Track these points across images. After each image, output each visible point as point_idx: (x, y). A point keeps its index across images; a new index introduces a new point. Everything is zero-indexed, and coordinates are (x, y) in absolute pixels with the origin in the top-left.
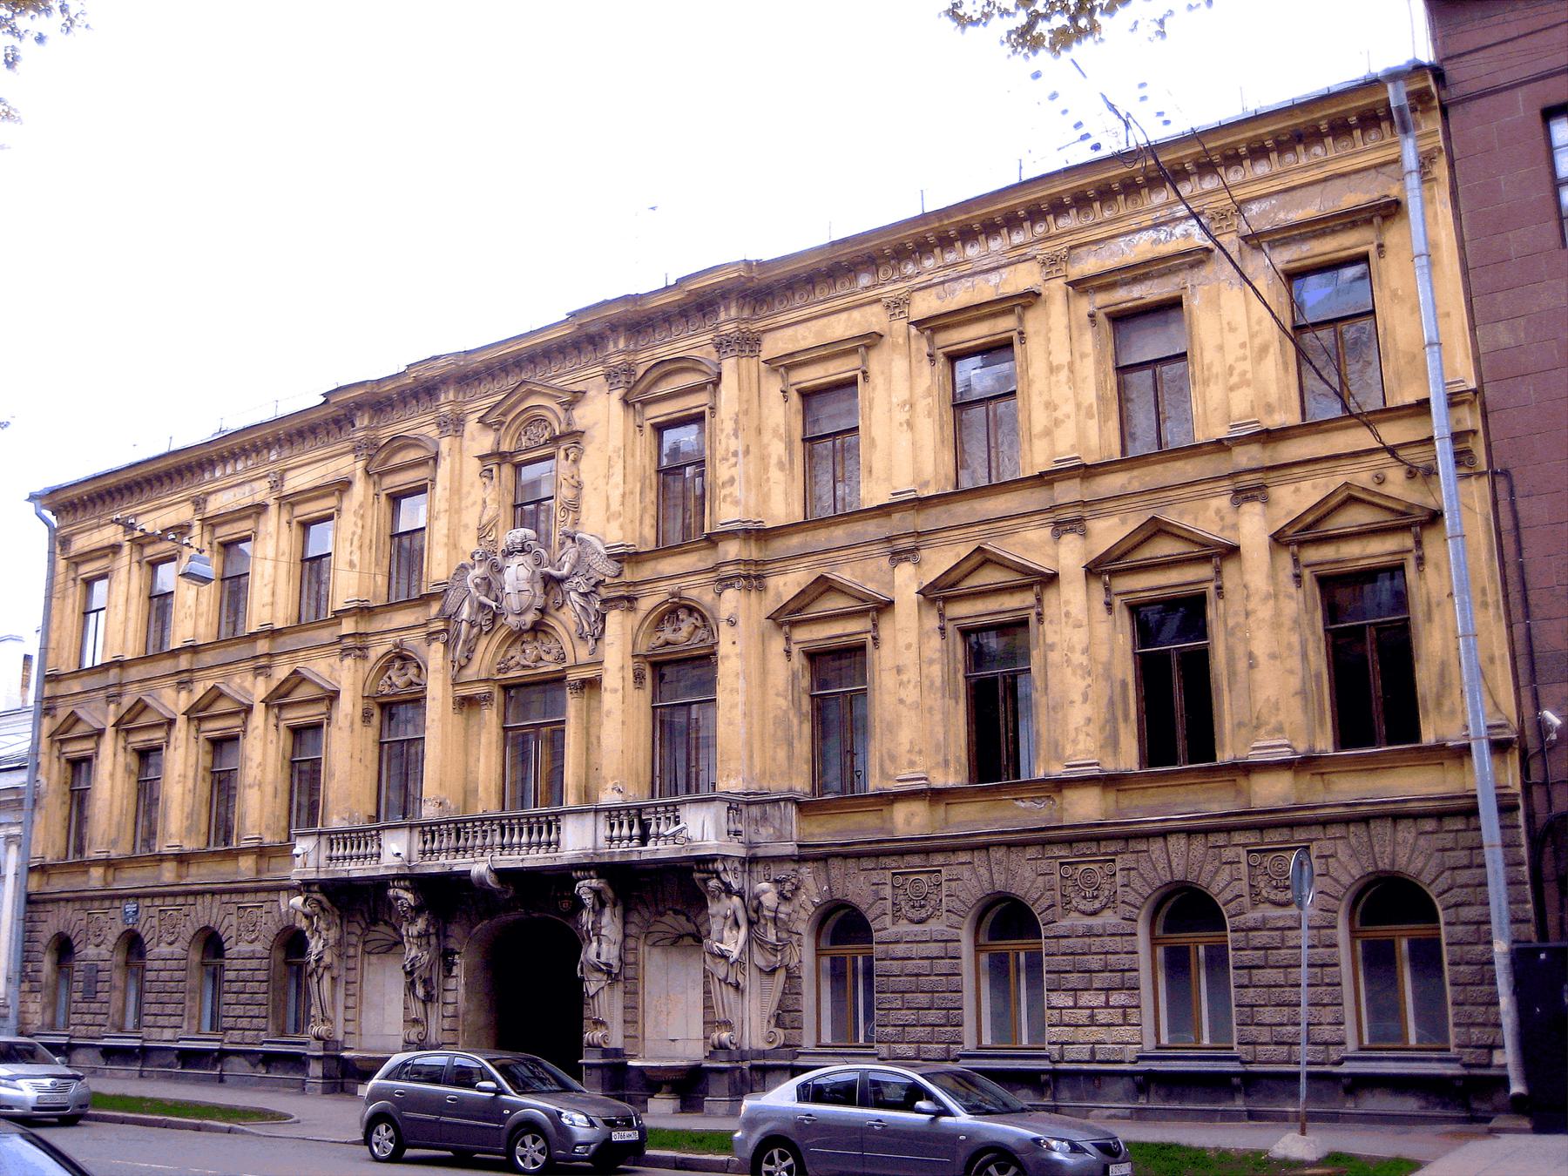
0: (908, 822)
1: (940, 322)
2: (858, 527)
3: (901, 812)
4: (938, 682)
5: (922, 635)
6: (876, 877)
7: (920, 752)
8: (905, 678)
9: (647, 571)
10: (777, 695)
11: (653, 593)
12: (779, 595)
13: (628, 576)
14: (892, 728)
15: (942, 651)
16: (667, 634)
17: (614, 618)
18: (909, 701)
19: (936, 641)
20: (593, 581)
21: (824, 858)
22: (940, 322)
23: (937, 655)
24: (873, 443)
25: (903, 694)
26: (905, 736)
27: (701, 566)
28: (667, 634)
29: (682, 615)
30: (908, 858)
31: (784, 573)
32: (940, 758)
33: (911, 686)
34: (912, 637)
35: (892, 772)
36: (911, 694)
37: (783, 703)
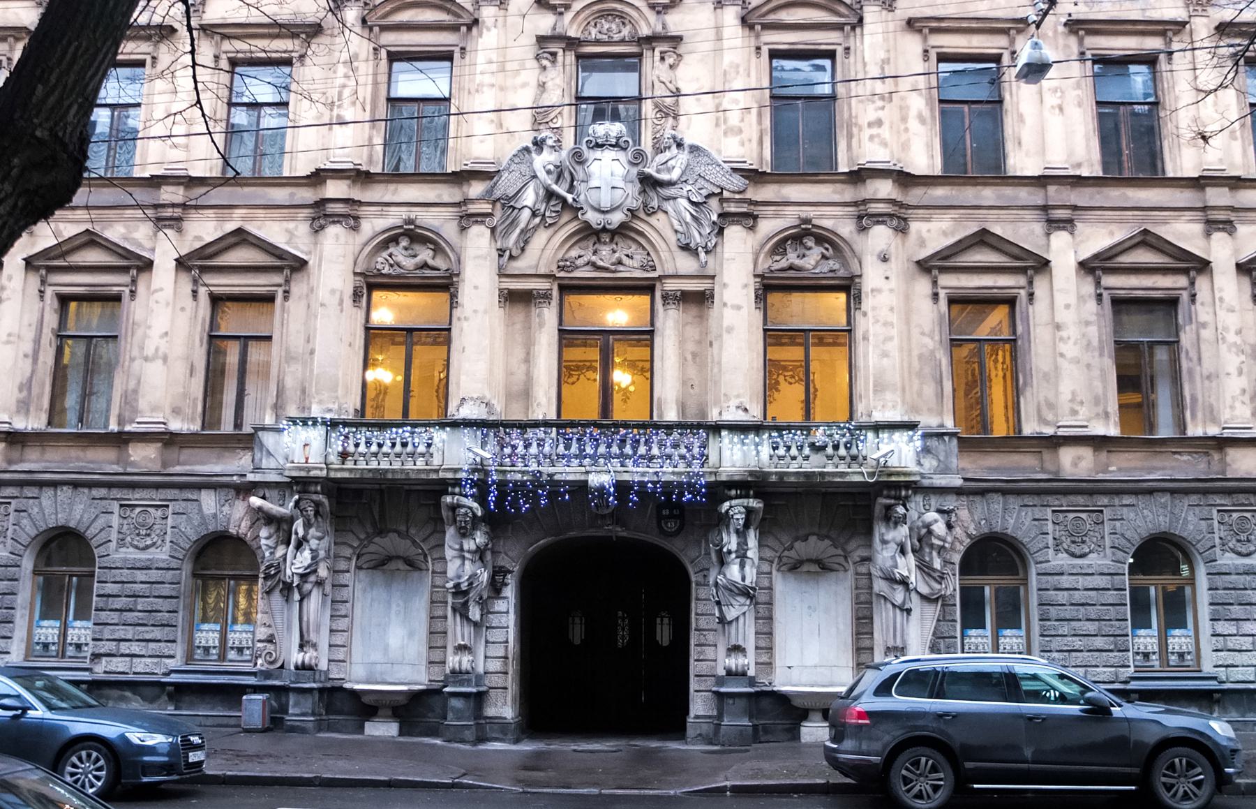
0: (1075, 465)
1: (1096, 26)
2: (1008, 191)
3: (1067, 456)
4: (1095, 342)
5: (1081, 298)
6: (1038, 513)
7: (1082, 403)
8: (1064, 334)
9: (767, 192)
10: (923, 334)
12: (922, 243)
13: (752, 194)
14: (1053, 377)
15: (1098, 314)
16: (792, 258)
17: (734, 233)
18: (1069, 355)
19: (1092, 305)
20: (704, 192)
21: (982, 493)
22: (1096, 26)
23: (1093, 318)
24: (1021, 119)
25: (1062, 348)
26: (1066, 387)
27: (837, 198)
28: (792, 258)
29: (810, 242)
30: (1072, 498)
31: (928, 220)
32: (1100, 409)
33: (1071, 342)
34: (1072, 300)
35: (1050, 417)
36: (1070, 350)
37: (930, 343)
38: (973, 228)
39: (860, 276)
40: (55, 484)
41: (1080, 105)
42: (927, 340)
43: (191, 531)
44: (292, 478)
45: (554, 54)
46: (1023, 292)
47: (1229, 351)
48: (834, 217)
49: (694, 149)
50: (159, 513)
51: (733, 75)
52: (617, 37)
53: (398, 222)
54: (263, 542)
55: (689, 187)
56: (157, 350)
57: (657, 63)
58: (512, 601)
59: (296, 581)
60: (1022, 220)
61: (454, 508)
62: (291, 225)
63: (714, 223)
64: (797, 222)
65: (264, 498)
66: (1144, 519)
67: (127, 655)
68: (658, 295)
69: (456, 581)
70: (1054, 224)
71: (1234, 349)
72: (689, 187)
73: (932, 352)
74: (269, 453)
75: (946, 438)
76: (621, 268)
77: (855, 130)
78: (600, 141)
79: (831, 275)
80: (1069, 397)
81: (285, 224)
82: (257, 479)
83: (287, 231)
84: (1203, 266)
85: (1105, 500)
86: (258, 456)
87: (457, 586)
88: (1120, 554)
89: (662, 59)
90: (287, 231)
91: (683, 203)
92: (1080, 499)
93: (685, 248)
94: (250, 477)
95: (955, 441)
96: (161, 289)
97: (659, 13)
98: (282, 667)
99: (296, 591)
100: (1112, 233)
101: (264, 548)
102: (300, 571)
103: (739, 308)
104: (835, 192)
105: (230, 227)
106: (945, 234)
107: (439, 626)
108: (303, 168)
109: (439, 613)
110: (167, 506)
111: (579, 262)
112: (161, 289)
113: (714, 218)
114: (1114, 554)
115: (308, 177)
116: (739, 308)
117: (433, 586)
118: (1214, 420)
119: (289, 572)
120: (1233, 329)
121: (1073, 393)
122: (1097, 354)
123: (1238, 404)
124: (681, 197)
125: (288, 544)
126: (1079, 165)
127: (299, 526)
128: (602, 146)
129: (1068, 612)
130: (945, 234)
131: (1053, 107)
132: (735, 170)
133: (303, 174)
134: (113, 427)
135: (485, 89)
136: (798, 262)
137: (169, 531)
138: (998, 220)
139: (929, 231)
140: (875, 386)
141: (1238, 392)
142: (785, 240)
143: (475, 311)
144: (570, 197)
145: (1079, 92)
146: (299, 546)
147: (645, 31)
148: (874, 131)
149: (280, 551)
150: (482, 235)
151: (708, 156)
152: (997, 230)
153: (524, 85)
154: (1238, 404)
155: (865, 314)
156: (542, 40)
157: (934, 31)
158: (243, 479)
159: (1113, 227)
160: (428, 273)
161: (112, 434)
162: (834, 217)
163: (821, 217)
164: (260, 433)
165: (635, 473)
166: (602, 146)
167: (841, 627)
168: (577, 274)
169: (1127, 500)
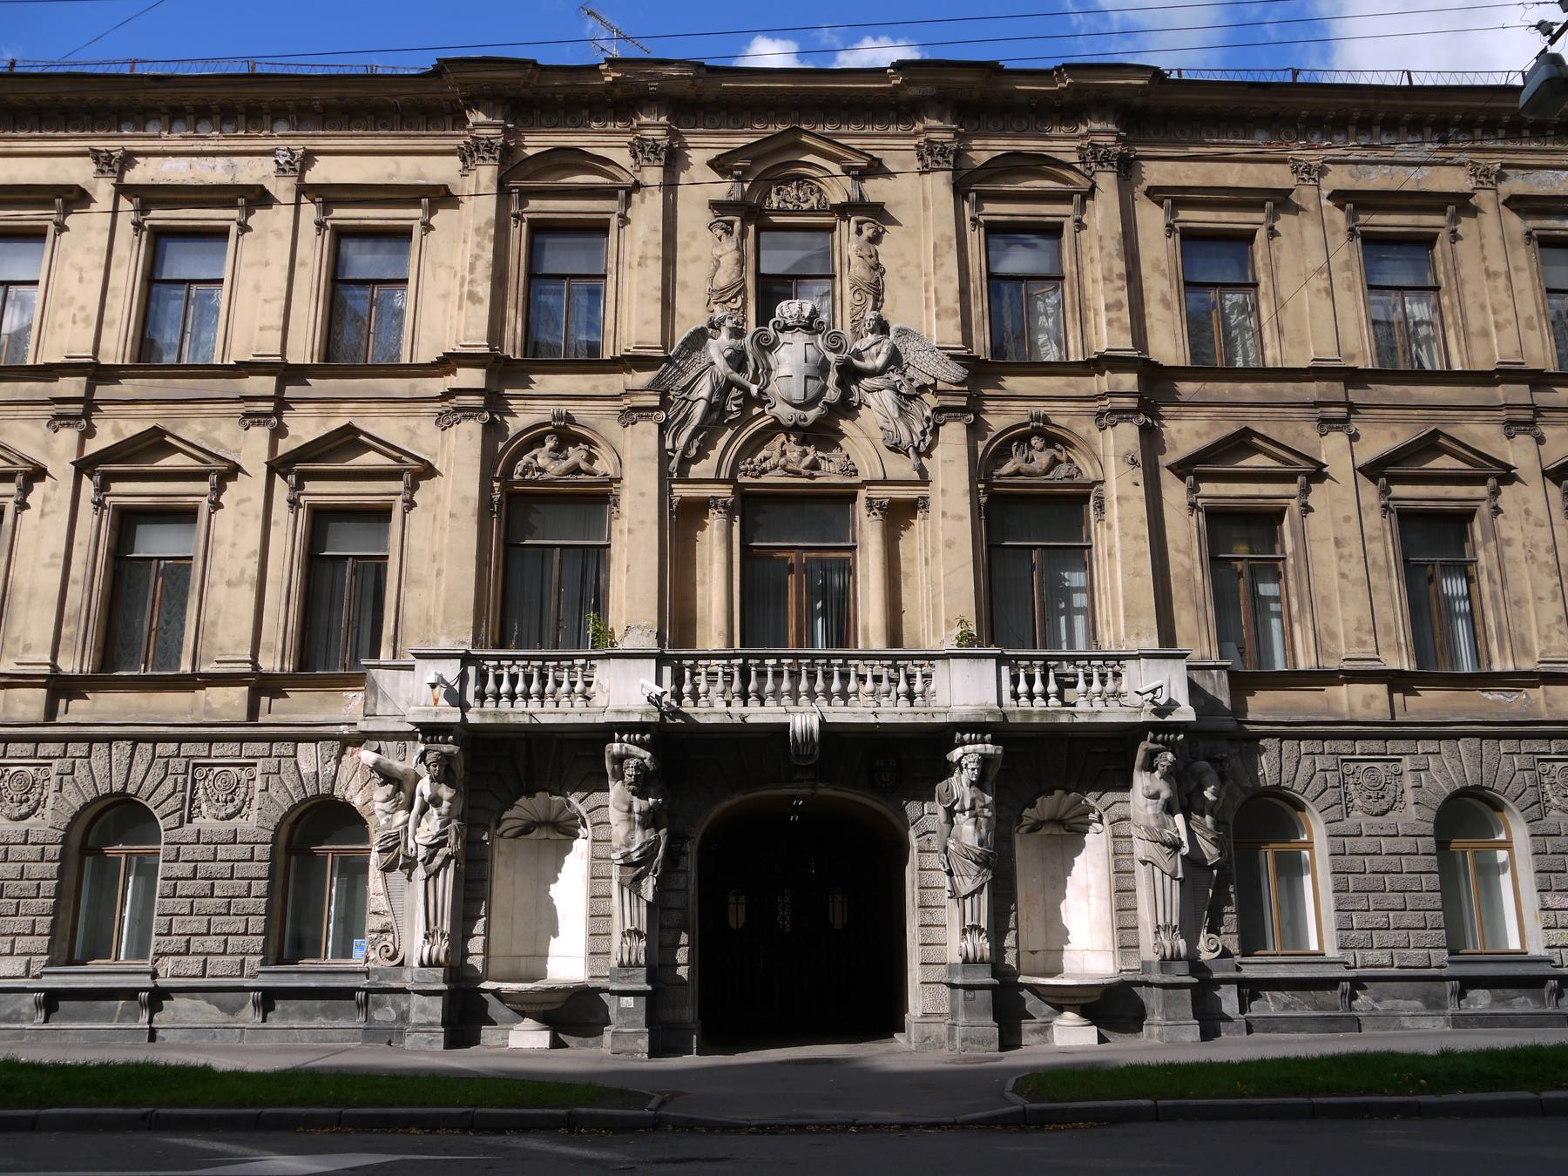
0: (1367, 705)
8: (1345, 551)
11: (1001, 412)
20: (916, 384)
25: (1345, 568)
38: (1230, 428)
39: (1102, 482)
40: (109, 739)
41: (1350, 288)
42: (1182, 558)
43: (283, 798)
44: (417, 724)
45: (731, 224)
46: (1294, 503)
47: (1540, 570)
48: (1069, 414)
49: (903, 332)
50: (244, 776)
51: (945, 249)
52: (805, 206)
53: (549, 418)
54: (378, 806)
55: (897, 378)
56: (243, 572)
57: (853, 236)
58: (693, 875)
59: (422, 853)
60: (1288, 419)
61: (619, 759)
62: (412, 422)
63: (928, 419)
64: (1027, 419)
65: (378, 751)
66: (1451, 768)
67: (200, 954)
68: (861, 503)
69: (625, 850)
70: (1327, 425)
71: (1546, 570)
72: (897, 378)
73: (1190, 572)
74: (385, 697)
75: (1215, 672)
76: (816, 473)
77: (1091, 315)
78: (789, 322)
79: (1067, 481)
80: (1355, 625)
81: (404, 421)
82: (370, 729)
83: (407, 429)
84: (1507, 475)
85: (1402, 746)
86: (371, 700)
87: (626, 856)
88: (1425, 811)
89: (859, 232)
90: (407, 429)
91: (888, 395)
92: (1375, 746)
93: (895, 448)
94: (363, 726)
95: (1225, 675)
96: (249, 499)
97: (854, 178)
98: (402, 964)
99: (420, 865)
100: (1394, 435)
101: (378, 813)
102: (427, 841)
103: (960, 518)
104: (1069, 385)
105: (336, 424)
106: (1198, 434)
107: (602, 906)
108: (426, 355)
109: (601, 890)
110: (255, 765)
111: (767, 465)
112: (249, 499)
113: (928, 413)
114: (1418, 812)
115: (433, 364)
116: (960, 518)
117: (594, 857)
118: (1527, 652)
119: (411, 844)
120: (1543, 546)
121: (1359, 621)
122: (1384, 575)
123: (1554, 634)
124: (889, 388)
125: (410, 808)
126: (1352, 357)
127: (425, 787)
128: (792, 328)
129: (1371, 880)
130: (1198, 434)
131: (1319, 290)
132: (953, 357)
133: (428, 361)
134: (185, 667)
135: (649, 262)
136: (1025, 467)
137: (257, 796)
138: (1260, 419)
139: (1179, 431)
140: (1126, 610)
141: (1554, 620)
142: (1009, 442)
143: (642, 522)
144: (754, 389)
145: (1349, 274)
146: (424, 810)
147: (837, 197)
148: (1113, 315)
149: (400, 816)
150: (650, 433)
151: (919, 338)
152: (1259, 429)
153: (697, 259)
154: (1554, 634)
155: (1110, 527)
156: (715, 205)
157: (1179, 204)
158: (353, 729)
159: (1396, 428)
160: (583, 478)
161: (184, 677)
162: (1069, 414)
163: (1055, 413)
164: (373, 671)
165: (840, 714)
166: (792, 328)
167: (1093, 901)
168: (764, 479)
169: (1432, 746)
